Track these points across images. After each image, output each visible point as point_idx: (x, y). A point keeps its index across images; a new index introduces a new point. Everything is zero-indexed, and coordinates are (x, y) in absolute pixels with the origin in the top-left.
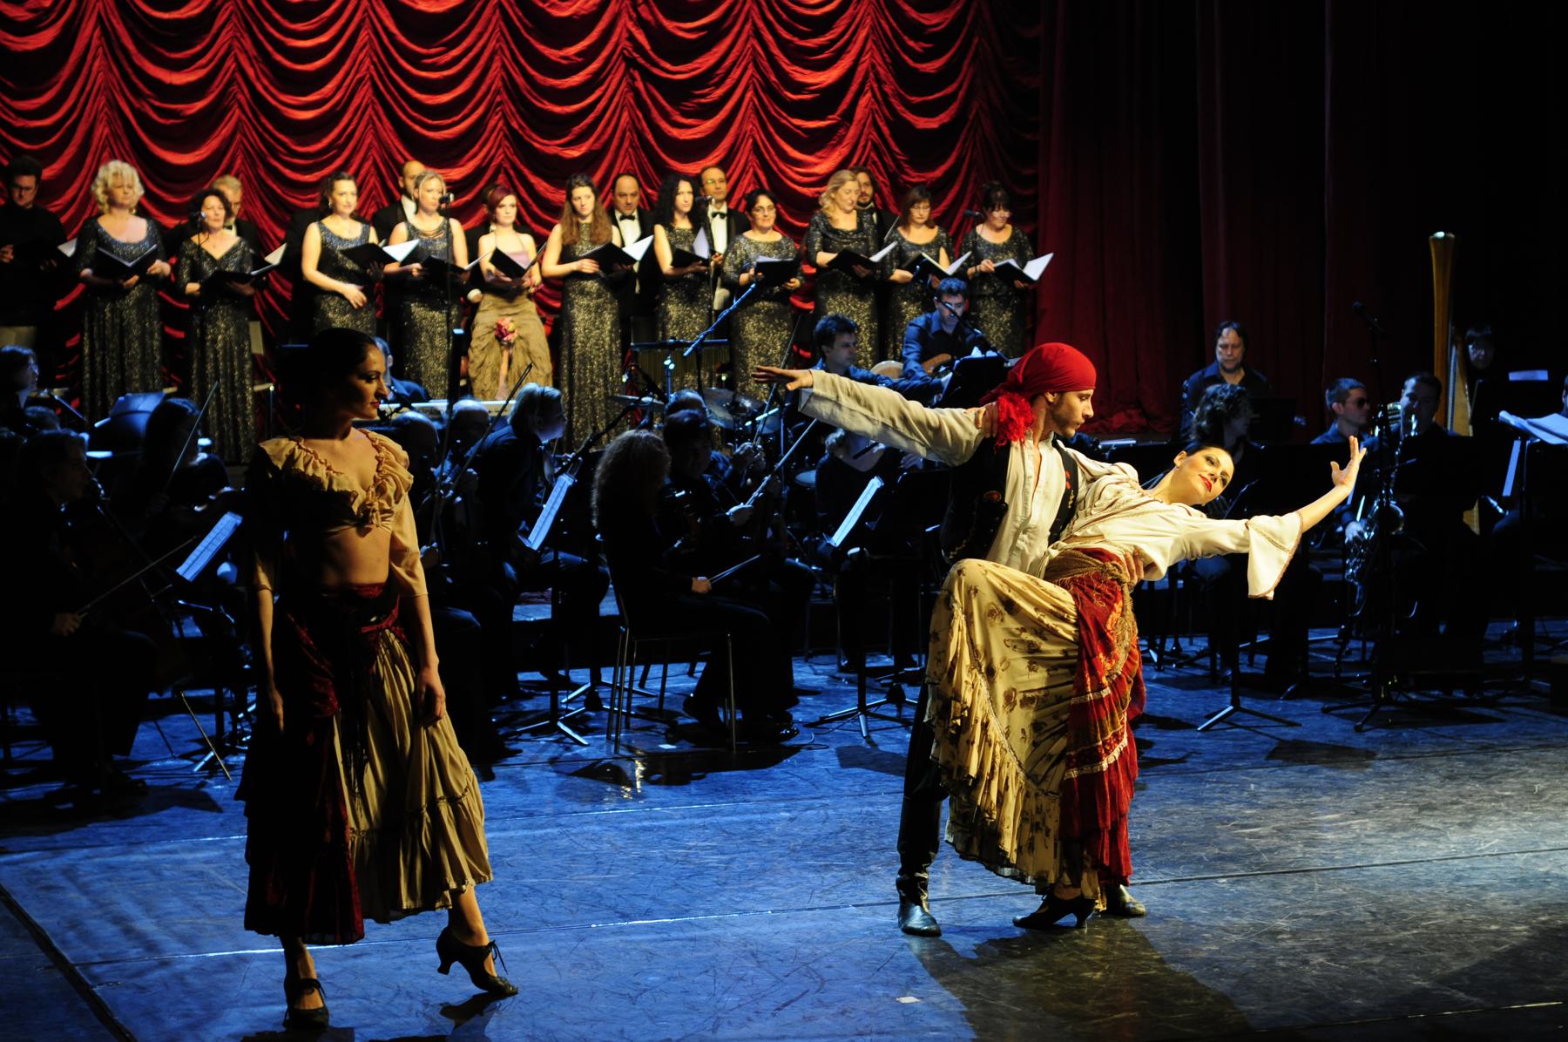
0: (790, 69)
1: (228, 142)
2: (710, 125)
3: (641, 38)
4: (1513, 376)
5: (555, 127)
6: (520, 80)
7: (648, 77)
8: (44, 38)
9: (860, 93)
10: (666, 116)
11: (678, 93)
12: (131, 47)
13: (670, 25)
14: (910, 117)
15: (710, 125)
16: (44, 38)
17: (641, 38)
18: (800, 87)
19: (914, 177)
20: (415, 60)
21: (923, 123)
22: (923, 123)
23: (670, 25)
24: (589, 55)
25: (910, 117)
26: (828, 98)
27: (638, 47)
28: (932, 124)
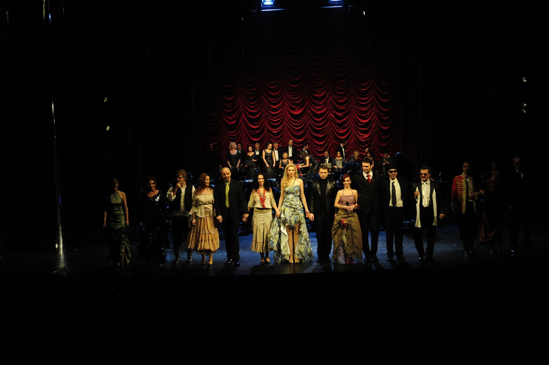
0: (359, 119)
1: (263, 137)
2: (345, 130)
3: (333, 116)
4: (228, 205)
5: (318, 132)
6: (312, 124)
7: (334, 123)
8: (234, 122)
9: (373, 123)
10: (338, 129)
11: (340, 125)
12: (247, 122)
13: (338, 114)
14: (382, 127)
15: (345, 130)
16: (234, 122)
17: (333, 116)
18: (362, 123)
19: (383, 138)
20: (294, 122)
21: (384, 128)
22: (384, 128)
23: (338, 114)
24: (324, 120)
25: (382, 127)
26: (366, 125)
27: (332, 118)
28: (386, 128)
